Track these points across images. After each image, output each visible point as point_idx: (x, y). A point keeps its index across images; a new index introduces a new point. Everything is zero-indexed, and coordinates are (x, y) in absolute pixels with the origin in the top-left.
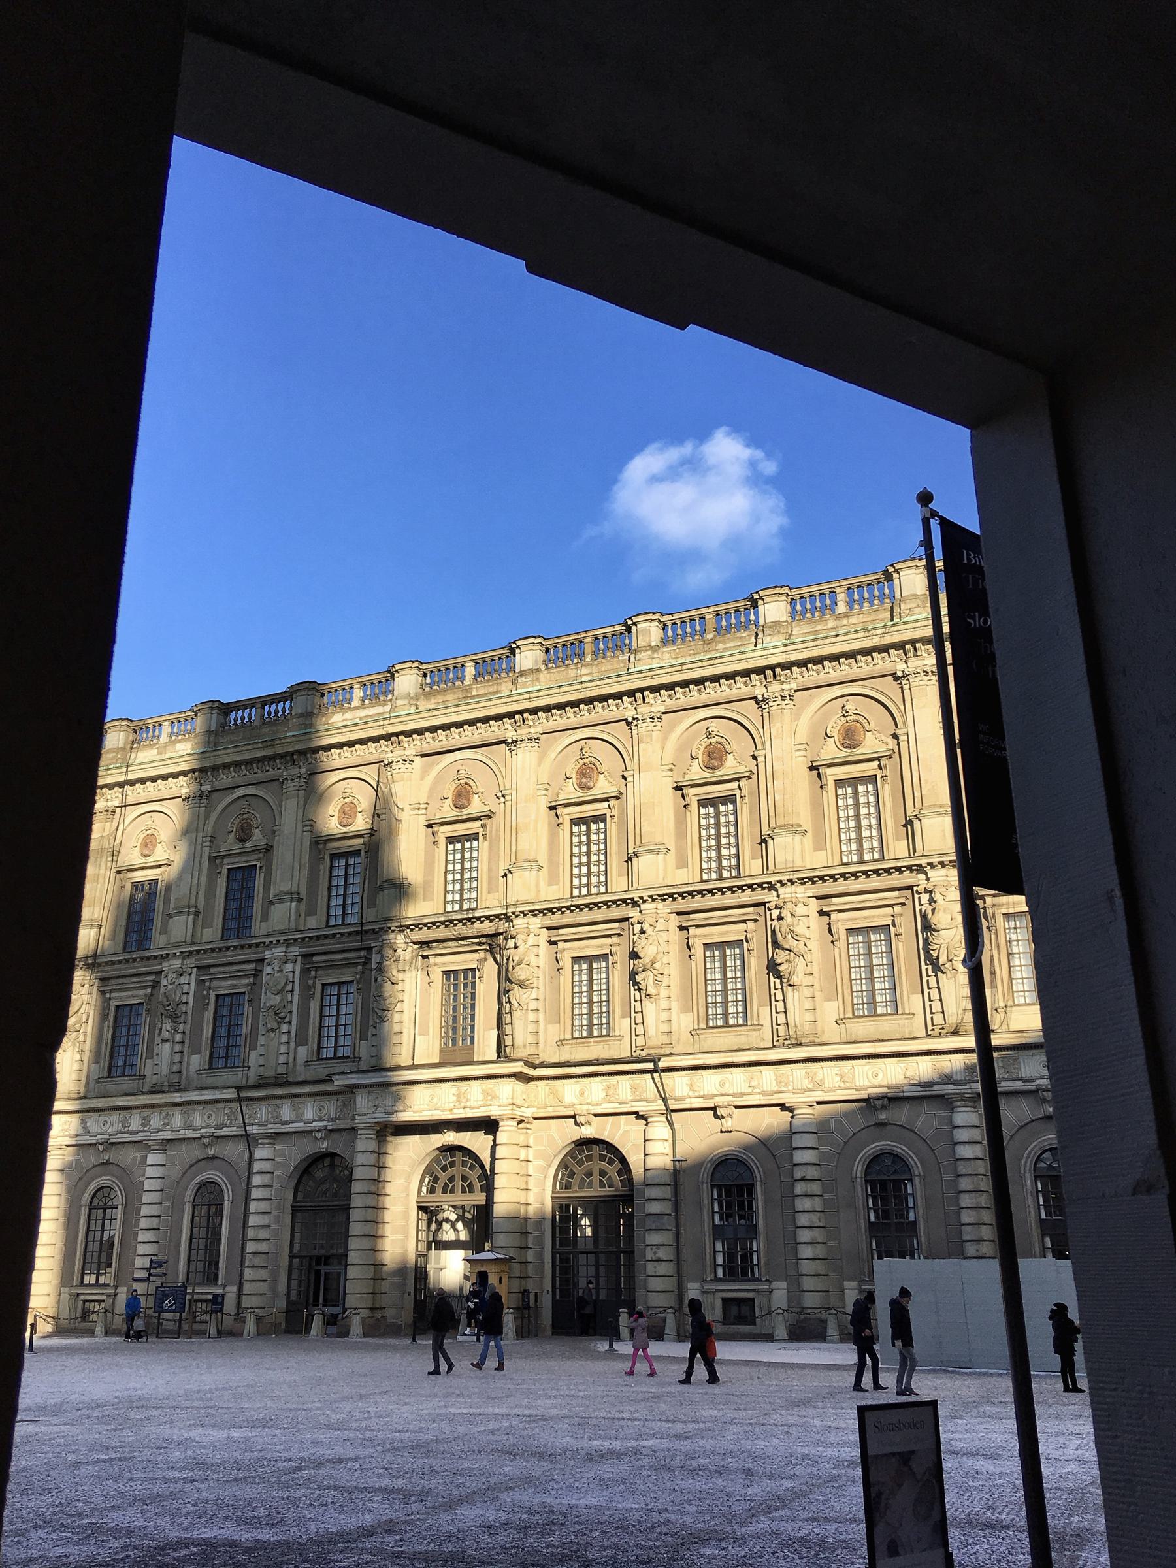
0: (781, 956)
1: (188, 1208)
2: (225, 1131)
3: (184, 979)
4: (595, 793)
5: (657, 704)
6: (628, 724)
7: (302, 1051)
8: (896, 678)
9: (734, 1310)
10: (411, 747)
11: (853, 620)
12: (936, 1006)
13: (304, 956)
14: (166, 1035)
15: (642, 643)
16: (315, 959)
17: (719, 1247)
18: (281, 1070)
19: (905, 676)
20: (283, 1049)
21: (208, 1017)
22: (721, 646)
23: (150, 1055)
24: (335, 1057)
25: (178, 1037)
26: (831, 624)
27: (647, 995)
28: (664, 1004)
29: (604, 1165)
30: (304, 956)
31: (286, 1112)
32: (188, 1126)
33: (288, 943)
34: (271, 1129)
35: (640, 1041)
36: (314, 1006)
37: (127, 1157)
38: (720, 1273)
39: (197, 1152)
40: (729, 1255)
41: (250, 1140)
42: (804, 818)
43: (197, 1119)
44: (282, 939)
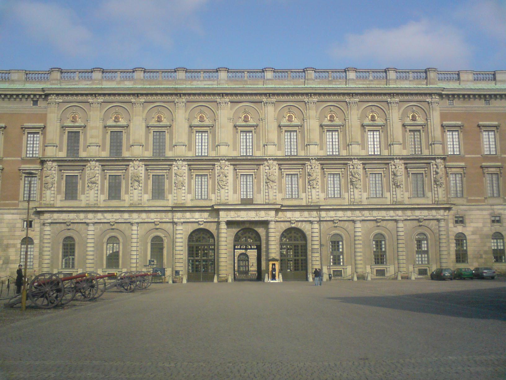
0: (354, 180)
1: (149, 245)
2: (164, 220)
3: (140, 168)
4: (293, 123)
5: (315, 99)
6: (306, 103)
7: (189, 197)
8: (388, 103)
9: (339, 273)
10: (227, 99)
11: (375, 82)
12: (395, 196)
13: (188, 165)
14: (136, 187)
15: (309, 77)
16: (192, 166)
17: (332, 257)
18: (183, 202)
19: (391, 103)
20: (183, 195)
21: (150, 182)
22: (334, 83)
23: (127, 192)
24: (202, 199)
25: (140, 188)
26: (368, 82)
27: (314, 188)
28: (317, 190)
29: (295, 235)
30: (188, 165)
31: (188, 215)
32: (148, 218)
33: (184, 160)
34: (182, 220)
35: (310, 200)
36: (193, 182)
37: (122, 227)
38: (332, 264)
39: (152, 226)
40: (334, 260)
41: (174, 223)
42: (359, 140)
43: (153, 215)
44: (182, 158)
